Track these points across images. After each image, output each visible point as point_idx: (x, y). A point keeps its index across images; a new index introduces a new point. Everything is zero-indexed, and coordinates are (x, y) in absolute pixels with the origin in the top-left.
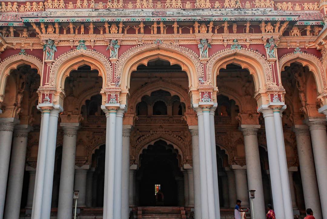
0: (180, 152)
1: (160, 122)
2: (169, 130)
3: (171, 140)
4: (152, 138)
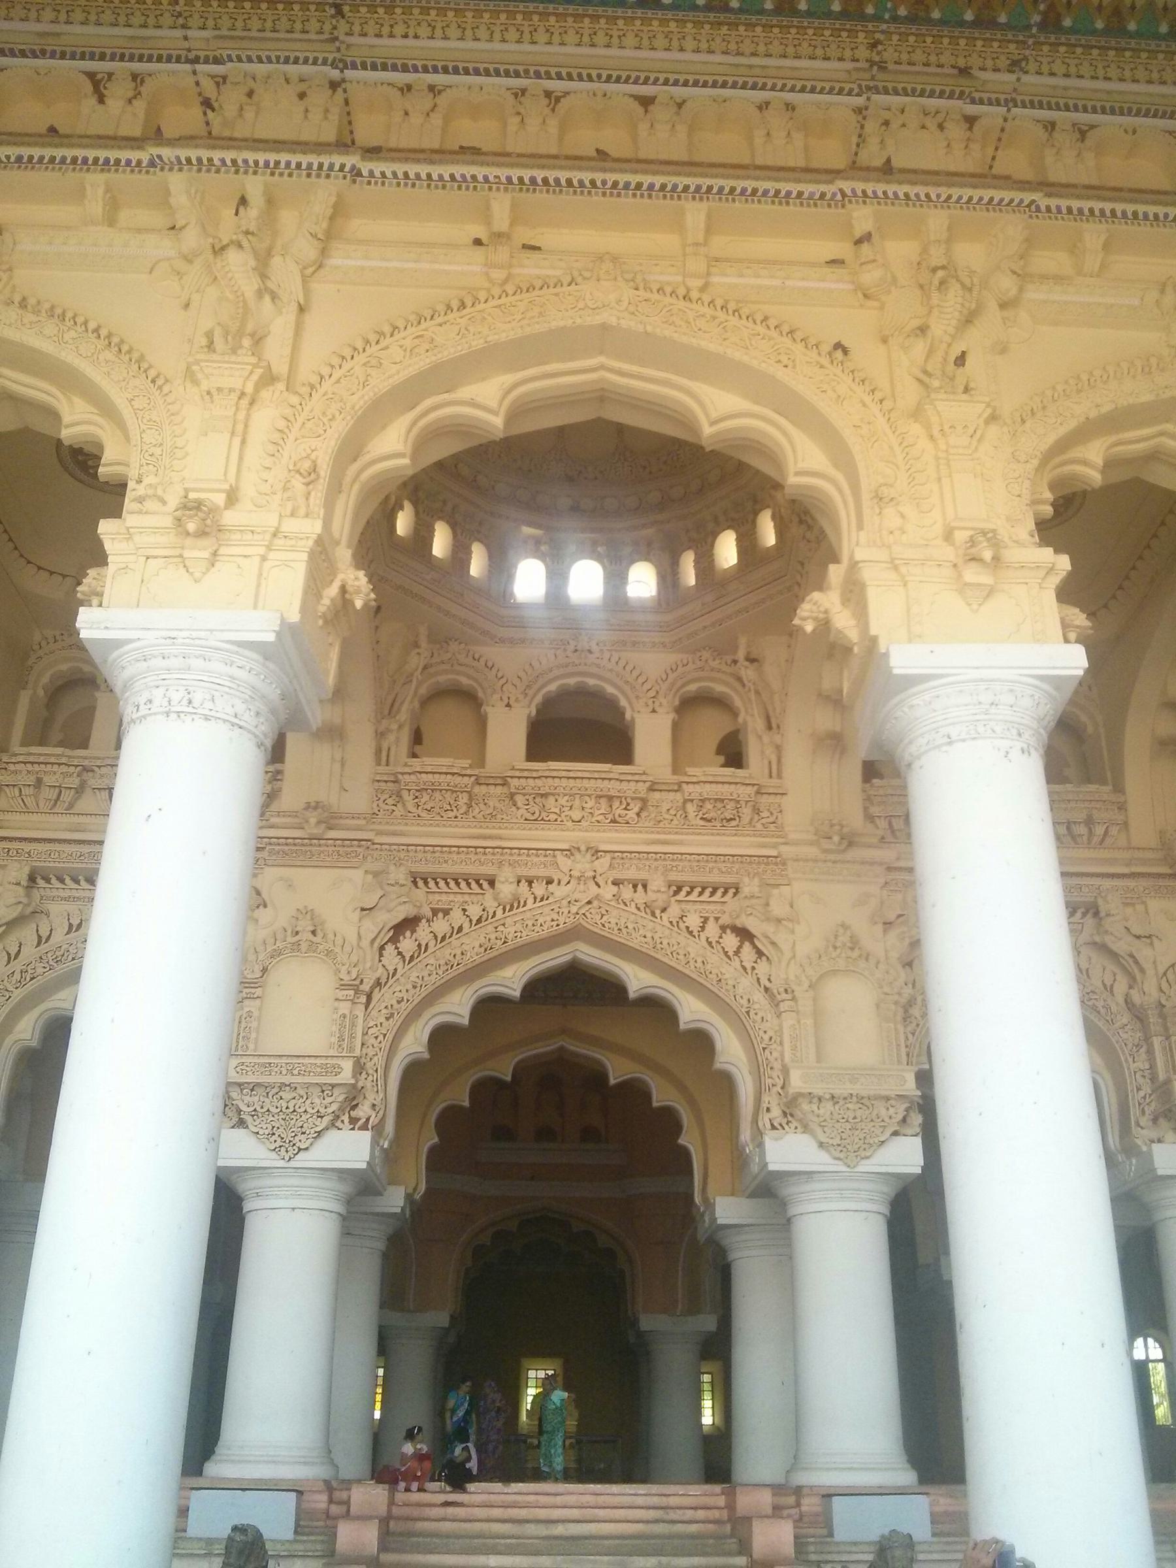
0: (731, 1051)
1: (576, 815)
2: (642, 875)
3: (655, 948)
4: (516, 929)
